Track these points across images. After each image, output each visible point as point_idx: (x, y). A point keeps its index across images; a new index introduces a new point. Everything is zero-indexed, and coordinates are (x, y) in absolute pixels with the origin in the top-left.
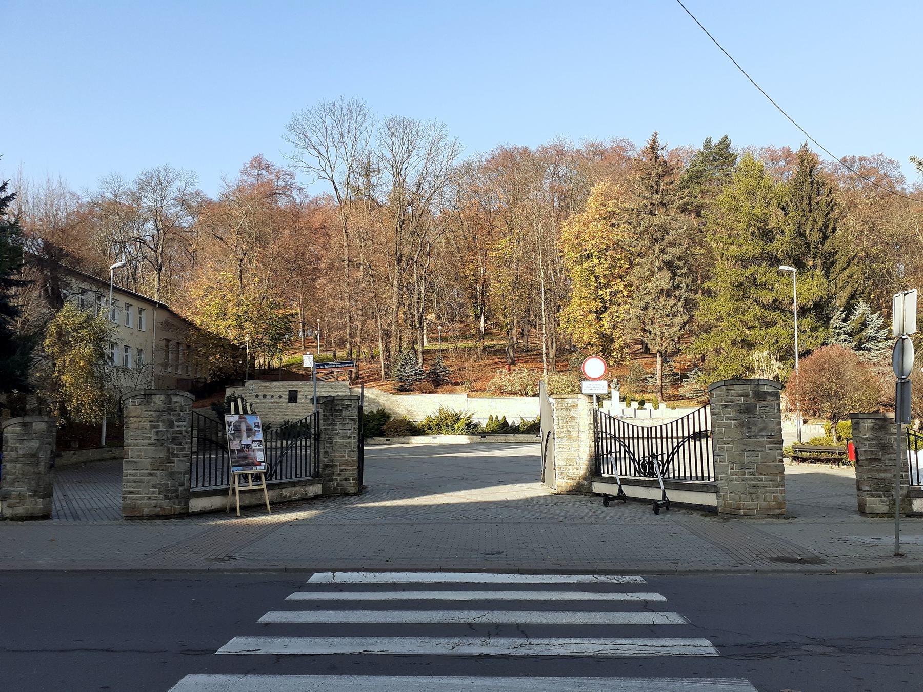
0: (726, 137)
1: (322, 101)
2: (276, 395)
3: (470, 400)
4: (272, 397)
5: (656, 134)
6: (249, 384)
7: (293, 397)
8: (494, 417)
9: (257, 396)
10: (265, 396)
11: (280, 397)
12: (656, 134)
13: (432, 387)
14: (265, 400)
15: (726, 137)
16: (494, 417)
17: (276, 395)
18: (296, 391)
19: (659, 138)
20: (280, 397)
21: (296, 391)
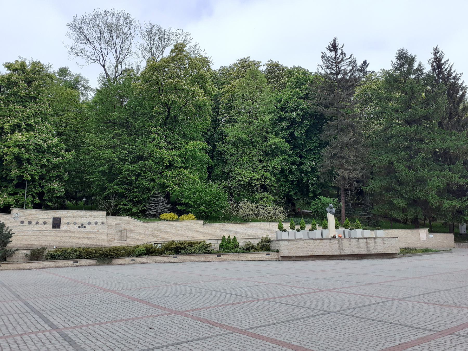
0: (366, 61)
1: (96, 10)
2: (41, 222)
3: (206, 226)
4: (37, 223)
5: (335, 39)
6: (15, 211)
7: (57, 223)
8: (227, 238)
9: (22, 222)
10: (30, 223)
11: (45, 223)
12: (335, 39)
13: (176, 216)
14: (30, 226)
15: (366, 61)
16: (227, 238)
17: (41, 222)
18: (59, 219)
19: (338, 42)
20: (45, 223)
21: (59, 219)
